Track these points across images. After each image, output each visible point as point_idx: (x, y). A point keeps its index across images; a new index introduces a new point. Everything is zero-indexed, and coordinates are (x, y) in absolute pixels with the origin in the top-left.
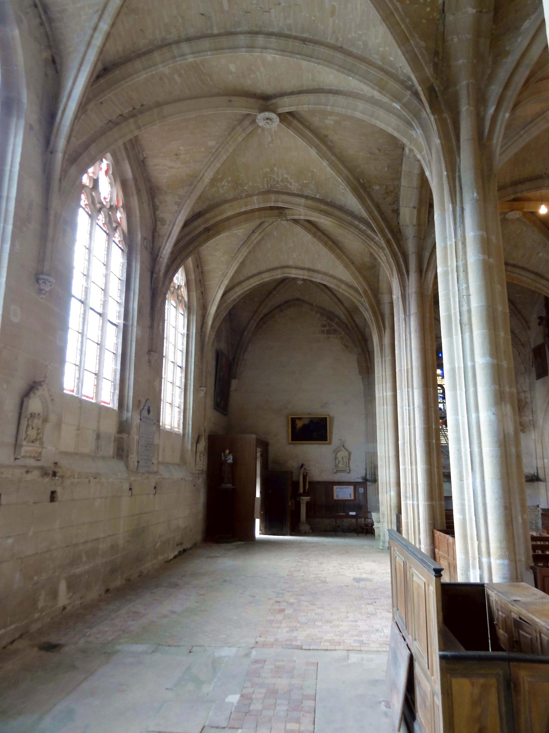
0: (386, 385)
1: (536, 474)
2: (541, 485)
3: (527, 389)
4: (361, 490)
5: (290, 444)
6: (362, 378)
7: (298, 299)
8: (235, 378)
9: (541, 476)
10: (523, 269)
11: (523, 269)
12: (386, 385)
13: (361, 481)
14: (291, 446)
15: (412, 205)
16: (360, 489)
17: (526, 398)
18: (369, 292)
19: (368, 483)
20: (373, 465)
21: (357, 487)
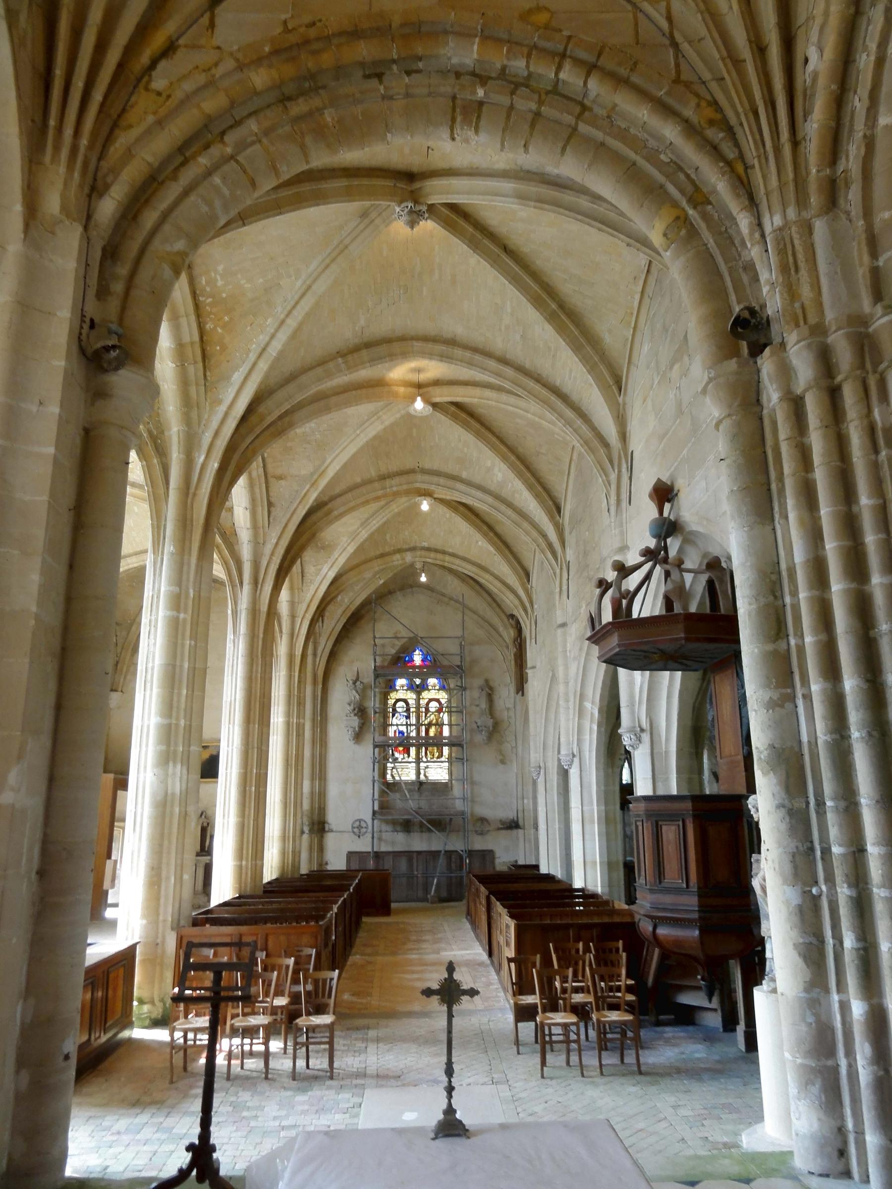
2: (520, 831)
3: (511, 706)
8: (116, 691)
9: (521, 823)
15: (244, 505)
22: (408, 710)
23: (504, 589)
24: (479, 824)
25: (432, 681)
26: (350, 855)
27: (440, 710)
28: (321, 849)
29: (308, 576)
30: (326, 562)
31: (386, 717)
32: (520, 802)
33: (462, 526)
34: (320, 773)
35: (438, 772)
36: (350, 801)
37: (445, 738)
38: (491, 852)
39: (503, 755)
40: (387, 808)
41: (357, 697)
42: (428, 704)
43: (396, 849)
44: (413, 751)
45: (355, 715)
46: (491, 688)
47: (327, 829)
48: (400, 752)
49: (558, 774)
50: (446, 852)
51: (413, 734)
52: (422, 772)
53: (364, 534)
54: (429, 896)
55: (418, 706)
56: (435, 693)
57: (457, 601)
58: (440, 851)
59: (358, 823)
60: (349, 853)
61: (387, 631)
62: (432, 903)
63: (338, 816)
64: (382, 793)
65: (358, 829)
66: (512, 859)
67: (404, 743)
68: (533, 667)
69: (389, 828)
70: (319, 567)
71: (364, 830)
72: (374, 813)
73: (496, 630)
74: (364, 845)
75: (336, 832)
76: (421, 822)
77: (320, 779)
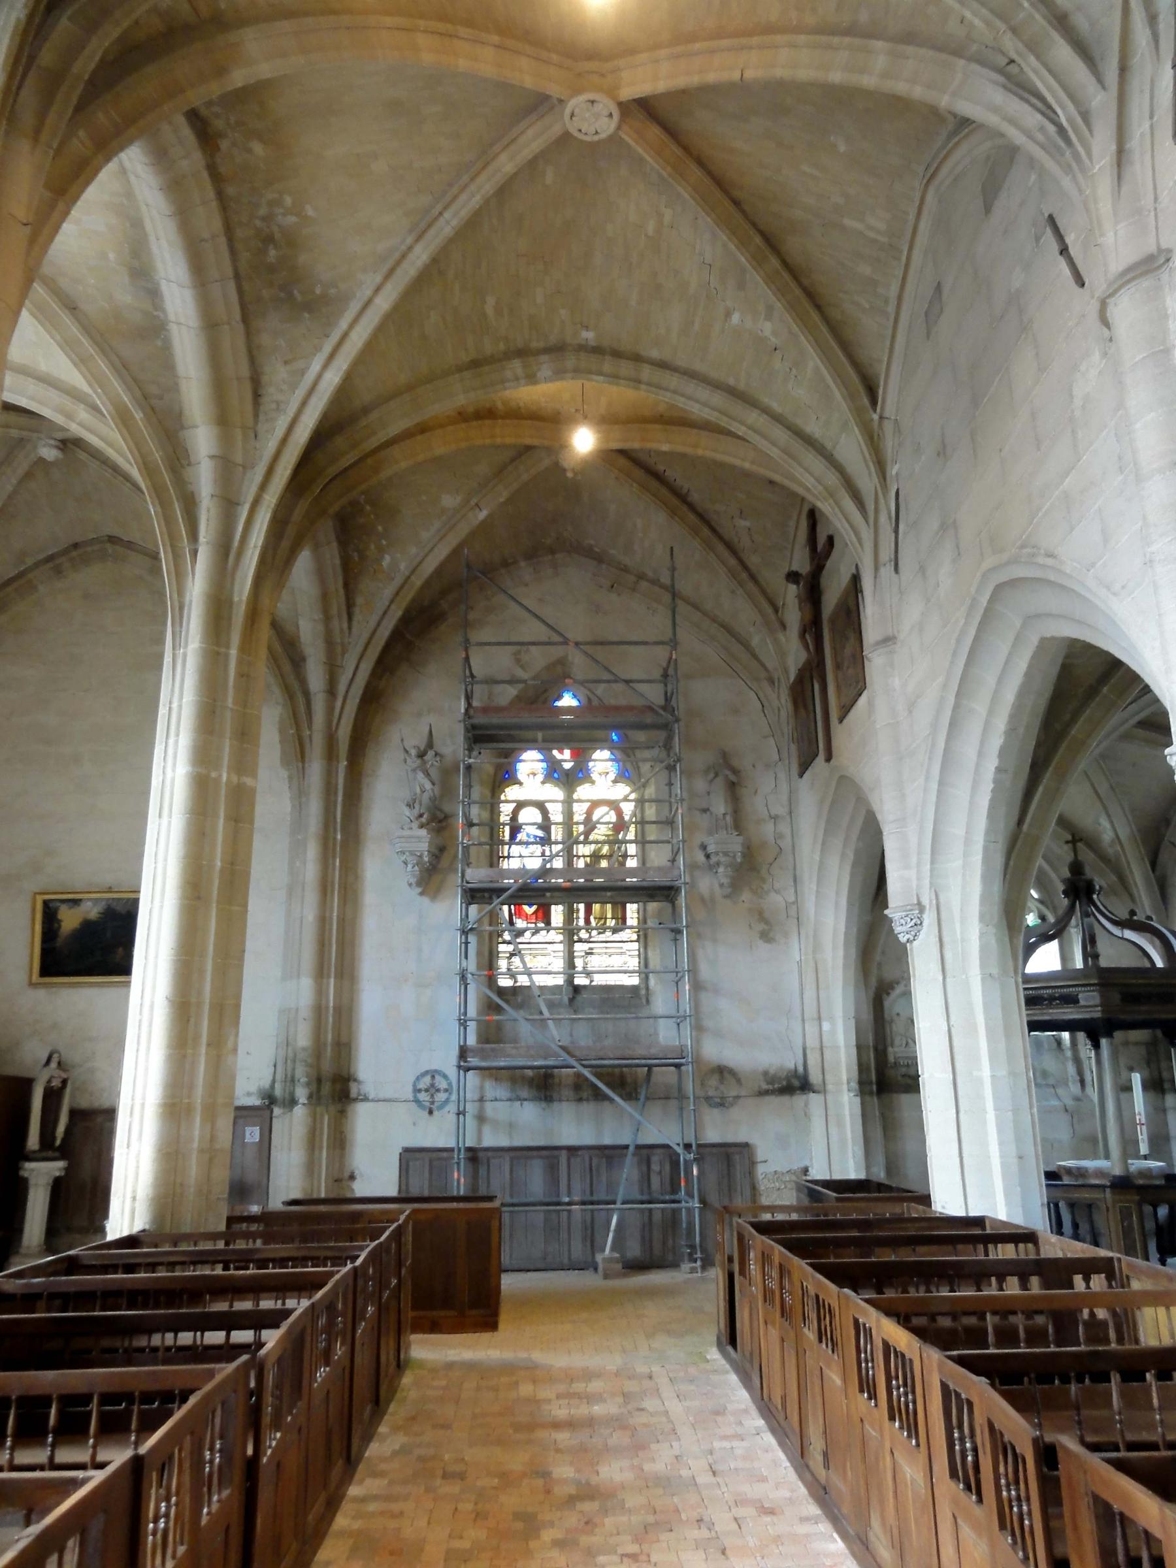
0: (177, 742)
1: (801, 1069)
3: (781, 810)
5: (31, 984)
6: (290, 778)
7: (112, 539)
9: (815, 1077)
11: (691, 375)
12: (177, 742)
13: (258, 1102)
14: (41, 993)
16: (248, 1130)
17: (779, 836)
18: (138, 416)
19: (277, 1111)
22: (546, 826)
23: (797, 446)
24: (713, 1081)
26: (409, 1156)
27: (620, 826)
28: (340, 1142)
29: (270, 393)
30: (318, 349)
31: (494, 841)
32: (811, 1029)
33: (697, 243)
34: (335, 955)
36: (409, 1029)
37: (632, 872)
38: (745, 1148)
39: (767, 922)
40: (499, 1041)
41: (428, 786)
42: (589, 813)
43: (518, 1142)
44: (557, 913)
45: (422, 826)
46: (735, 772)
47: (353, 1094)
48: (526, 917)
49: (982, 918)
50: (638, 1147)
51: (558, 864)
52: (579, 963)
53: (421, 256)
54: (599, 1258)
55: (569, 814)
56: (605, 782)
57: (655, 582)
58: (627, 1147)
59: (427, 1080)
60: (407, 1150)
61: (494, 652)
62: (606, 1276)
63: (381, 1065)
64: (490, 1007)
65: (427, 1094)
66: (797, 1165)
67: (536, 893)
68: (888, 640)
69: (502, 1091)
70: (300, 364)
71: (441, 1097)
72: (463, 1052)
73: (746, 646)
74: (437, 1133)
75: (373, 1101)
76: (578, 1075)
77: (340, 975)
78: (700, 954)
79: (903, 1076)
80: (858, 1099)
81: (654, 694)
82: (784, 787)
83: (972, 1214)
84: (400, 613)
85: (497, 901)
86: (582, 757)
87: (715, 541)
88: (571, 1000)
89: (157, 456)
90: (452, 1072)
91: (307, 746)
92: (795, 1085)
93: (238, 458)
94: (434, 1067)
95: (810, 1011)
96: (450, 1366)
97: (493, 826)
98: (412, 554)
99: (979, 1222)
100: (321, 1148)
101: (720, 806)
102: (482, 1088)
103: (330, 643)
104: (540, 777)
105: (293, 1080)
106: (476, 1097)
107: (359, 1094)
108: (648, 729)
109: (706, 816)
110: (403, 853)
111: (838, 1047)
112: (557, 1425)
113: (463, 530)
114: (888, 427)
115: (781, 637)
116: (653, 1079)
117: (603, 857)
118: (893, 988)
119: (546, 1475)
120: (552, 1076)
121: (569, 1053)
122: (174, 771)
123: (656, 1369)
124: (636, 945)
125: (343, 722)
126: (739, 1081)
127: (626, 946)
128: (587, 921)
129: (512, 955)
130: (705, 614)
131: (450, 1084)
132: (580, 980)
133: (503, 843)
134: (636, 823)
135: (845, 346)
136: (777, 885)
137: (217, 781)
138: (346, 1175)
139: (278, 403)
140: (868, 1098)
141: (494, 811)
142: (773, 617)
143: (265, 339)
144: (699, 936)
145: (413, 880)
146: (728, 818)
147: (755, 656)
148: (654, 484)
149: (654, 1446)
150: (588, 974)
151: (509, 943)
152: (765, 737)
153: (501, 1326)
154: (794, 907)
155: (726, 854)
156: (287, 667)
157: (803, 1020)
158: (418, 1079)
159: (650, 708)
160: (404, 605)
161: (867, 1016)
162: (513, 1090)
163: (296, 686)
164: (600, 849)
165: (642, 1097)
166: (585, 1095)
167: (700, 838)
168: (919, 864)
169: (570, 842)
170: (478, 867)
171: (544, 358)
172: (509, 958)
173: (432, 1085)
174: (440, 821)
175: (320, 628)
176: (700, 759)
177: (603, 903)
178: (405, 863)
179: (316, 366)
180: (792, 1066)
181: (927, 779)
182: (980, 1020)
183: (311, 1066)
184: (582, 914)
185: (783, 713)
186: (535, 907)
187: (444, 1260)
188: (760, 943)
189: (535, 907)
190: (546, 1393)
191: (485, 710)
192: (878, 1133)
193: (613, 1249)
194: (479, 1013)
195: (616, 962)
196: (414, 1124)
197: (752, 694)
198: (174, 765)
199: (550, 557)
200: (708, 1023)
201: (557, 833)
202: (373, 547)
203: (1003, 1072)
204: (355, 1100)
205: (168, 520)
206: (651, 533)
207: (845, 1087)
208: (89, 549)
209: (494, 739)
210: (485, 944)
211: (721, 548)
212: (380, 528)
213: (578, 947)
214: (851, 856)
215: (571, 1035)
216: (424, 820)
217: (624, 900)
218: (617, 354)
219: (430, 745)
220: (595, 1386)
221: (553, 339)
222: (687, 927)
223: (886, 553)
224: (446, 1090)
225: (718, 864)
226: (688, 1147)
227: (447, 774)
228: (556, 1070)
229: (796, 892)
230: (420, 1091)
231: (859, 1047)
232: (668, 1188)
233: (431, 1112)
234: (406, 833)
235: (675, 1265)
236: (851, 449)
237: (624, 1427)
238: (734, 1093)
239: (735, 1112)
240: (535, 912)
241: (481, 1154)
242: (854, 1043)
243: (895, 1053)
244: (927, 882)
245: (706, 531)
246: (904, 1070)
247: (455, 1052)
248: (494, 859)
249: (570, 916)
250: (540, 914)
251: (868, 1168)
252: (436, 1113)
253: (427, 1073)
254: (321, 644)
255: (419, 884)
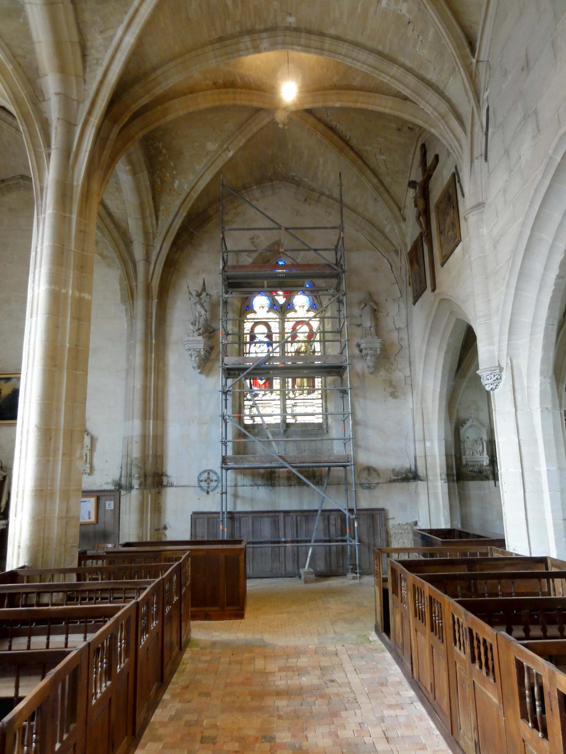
0: (40, 272)
1: (413, 468)
3: (402, 325)
4: (110, 505)
6: (126, 310)
9: (421, 472)
10: (356, 44)
11: (356, 44)
12: (40, 272)
13: (112, 488)
16: (107, 503)
18: (10, 67)
19: (123, 492)
20: (129, 459)
21: (102, 499)
22: (269, 335)
24: (365, 475)
25: (301, 301)
26: (196, 517)
27: (311, 335)
28: (158, 509)
29: (93, 54)
30: (120, 22)
31: (241, 343)
32: (419, 446)
34: (153, 406)
35: (308, 407)
37: (318, 358)
39: (394, 387)
41: (203, 312)
43: (256, 509)
44: (277, 383)
45: (200, 335)
46: (376, 304)
47: (165, 483)
49: (542, 373)
50: (323, 511)
52: (289, 411)
54: (302, 571)
55: (282, 329)
57: (330, 197)
58: (317, 511)
59: (206, 475)
62: (306, 582)
64: (241, 435)
65: (206, 483)
67: (263, 371)
68: (480, 205)
69: (248, 481)
70: (110, 33)
71: (213, 484)
72: (224, 460)
73: (382, 233)
74: (211, 504)
75: (176, 486)
76: (289, 472)
78: (357, 406)
79: (470, 471)
80: (447, 484)
81: (330, 257)
82: (404, 312)
83: (534, 555)
84: (185, 214)
85: (243, 375)
86: (289, 296)
87: (365, 168)
88: (285, 431)
89: (23, 94)
90: (218, 471)
91: (135, 293)
92: (411, 476)
93: (74, 95)
94: (208, 468)
95: (419, 435)
96: (214, 644)
97: (240, 334)
98: (191, 179)
99: (543, 560)
100: (147, 512)
101: (368, 323)
102: (236, 480)
103: (146, 233)
104: (266, 309)
105: (131, 476)
106: (233, 484)
107: (168, 483)
108: (325, 279)
109: (359, 329)
110: (189, 350)
111: (434, 456)
112: (279, 694)
113: (220, 163)
114: (482, 67)
115: (402, 224)
116: (331, 473)
117: (301, 352)
118: (465, 423)
119: (271, 739)
120: (274, 472)
121: (284, 459)
122: (39, 289)
123: (339, 648)
124: (320, 401)
125: (155, 276)
126: (379, 475)
127: (315, 401)
128: (293, 386)
129: (252, 407)
130: (359, 214)
131: (218, 477)
132: (290, 420)
133: (246, 343)
134: (320, 332)
135: (456, 14)
136: (399, 367)
137: (66, 295)
138: (162, 527)
139: (97, 60)
140: (451, 484)
141: (241, 327)
142: (398, 214)
143: (87, 16)
144: (356, 395)
145: (196, 365)
146: (372, 329)
147: (387, 238)
148: (331, 133)
149: (343, 714)
150: (294, 416)
151: (250, 400)
152: (393, 284)
153: (246, 615)
154: (409, 379)
155: (371, 349)
156: (122, 246)
157: (415, 441)
158: (200, 475)
159: (329, 265)
160: (187, 209)
161: (451, 439)
162: (253, 480)
163: (127, 257)
164: (300, 348)
165: (325, 485)
166: (293, 483)
167: (355, 341)
168: (500, 341)
169: (283, 343)
170: (232, 356)
171: (264, 35)
172: (250, 409)
173: (208, 478)
174: (210, 333)
175: (140, 223)
176: (356, 297)
177: (302, 378)
178: (191, 356)
179: (120, 32)
180: (408, 466)
181: (508, 286)
182: (540, 436)
183: (140, 468)
184: (290, 384)
185: (403, 270)
186: (264, 381)
187: (212, 578)
188: (391, 398)
189: (264, 381)
190: (272, 667)
191: (234, 267)
192: (457, 502)
193: (310, 566)
194: (234, 438)
195: (310, 410)
196: (199, 499)
197: (385, 261)
198: (39, 285)
199: (270, 184)
200: (361, 443)
201: (276, 338)
202: (168, 174)
203: (554, 468)
204: (166, 486)
205: (32, 136)
206: (328, 166)
207: (439, 477)
208: (10, 183)
209: (239, 286)
210: (237, 401)
211: (368, 172)
212: (172, 164)
213: (288, 402)
214: (445, 347)
215: (285, 450)
216: (201, 331)
217: (313, 375)
218: (309, 32)
219: (204, 289)
220: (303, 661)
221: (269, 24)
222: (351, 388)
223: (479, 149)
224: (216, 481)
225: (367, 355)
226: (351, 511)
227: (214, 306)
228: (277, 470)
229: (410, 370)
230: (201, 481)
231: (447, 455)
232: (339, 532)
233: (208, 493)
234: (191, 338)
235: (343, 575)
236: (457, 87)
237: (322, 696)
238: (376, 481)
239: (377, 492)
240: (265, 383)
241: (236, 515)
242: (444, 453)
243: (466, 459)
244: (505, 352)
245: (360, 162)
246: (471, 468)
247: (220, 460)
248: (241, 353)
249: (284, 384)
250: (267, 385)
251: (452, 522)
252: (210, 493)
253: (205, 471)
254: (140, 232)
255: (199, 367)
